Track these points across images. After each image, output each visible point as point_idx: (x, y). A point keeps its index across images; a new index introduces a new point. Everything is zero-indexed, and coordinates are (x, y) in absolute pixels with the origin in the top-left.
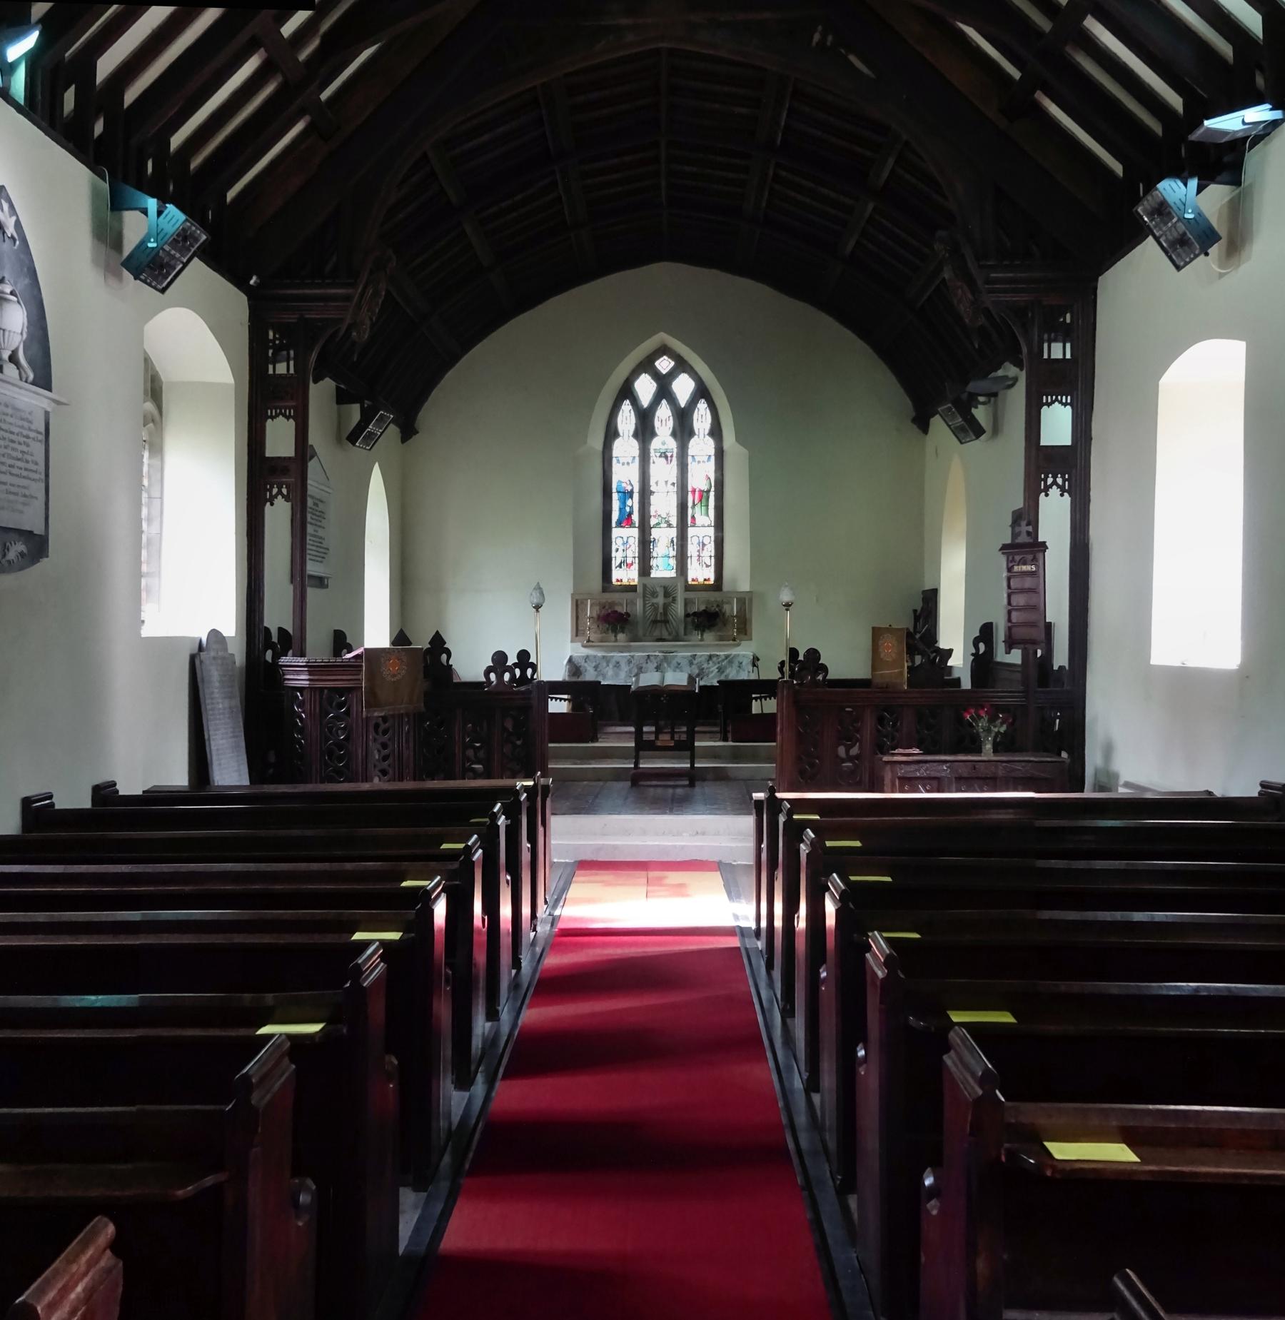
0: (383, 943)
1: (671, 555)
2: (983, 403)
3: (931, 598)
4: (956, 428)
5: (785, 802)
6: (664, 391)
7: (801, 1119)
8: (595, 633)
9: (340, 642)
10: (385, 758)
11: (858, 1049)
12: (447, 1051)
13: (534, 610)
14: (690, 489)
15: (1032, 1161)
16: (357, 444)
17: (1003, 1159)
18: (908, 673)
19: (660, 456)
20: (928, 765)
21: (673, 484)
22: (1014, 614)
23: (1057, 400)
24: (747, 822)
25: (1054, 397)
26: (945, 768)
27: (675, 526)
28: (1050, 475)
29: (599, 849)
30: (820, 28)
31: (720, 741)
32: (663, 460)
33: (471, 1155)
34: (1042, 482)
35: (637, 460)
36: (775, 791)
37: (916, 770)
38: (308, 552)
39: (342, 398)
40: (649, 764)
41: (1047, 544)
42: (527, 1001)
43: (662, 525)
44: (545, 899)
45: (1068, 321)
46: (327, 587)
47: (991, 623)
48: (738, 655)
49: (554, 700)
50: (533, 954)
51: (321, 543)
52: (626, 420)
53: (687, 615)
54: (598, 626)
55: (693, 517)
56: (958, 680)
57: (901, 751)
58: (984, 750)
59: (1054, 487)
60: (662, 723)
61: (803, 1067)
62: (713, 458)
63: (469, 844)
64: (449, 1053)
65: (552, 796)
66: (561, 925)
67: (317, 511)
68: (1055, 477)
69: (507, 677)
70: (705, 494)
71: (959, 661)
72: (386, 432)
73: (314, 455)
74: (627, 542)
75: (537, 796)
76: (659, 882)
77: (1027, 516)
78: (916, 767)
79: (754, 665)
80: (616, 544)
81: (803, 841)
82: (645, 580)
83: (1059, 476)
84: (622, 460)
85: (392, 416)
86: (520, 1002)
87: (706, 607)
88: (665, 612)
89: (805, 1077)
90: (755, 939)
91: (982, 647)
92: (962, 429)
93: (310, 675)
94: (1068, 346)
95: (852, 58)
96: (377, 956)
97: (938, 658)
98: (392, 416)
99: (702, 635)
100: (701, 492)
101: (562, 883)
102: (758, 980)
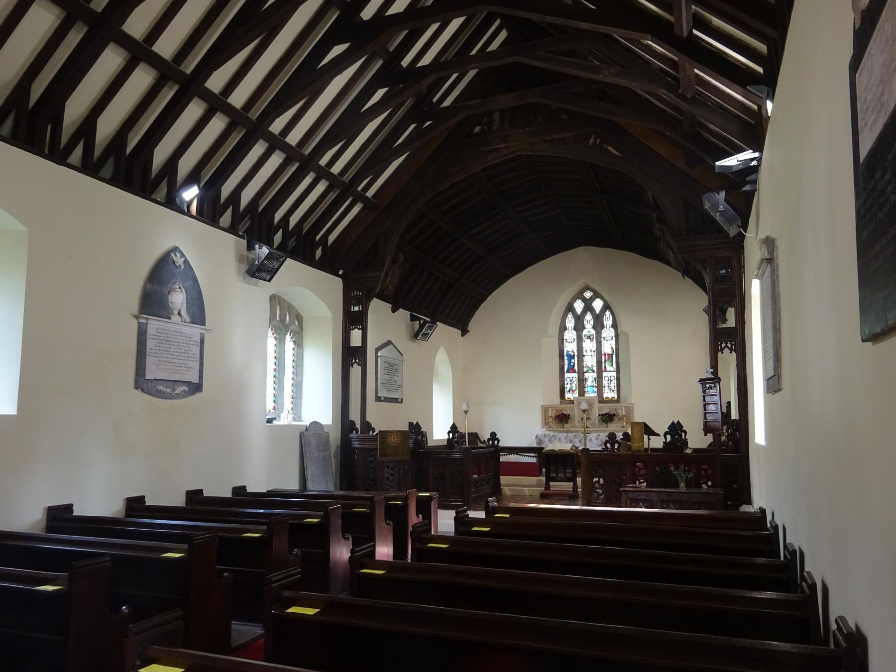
6: (588, 308)
19: (587, 338)
21: (594, 351)
32: (589, 340)
35: (576, 340)
55: (605, 367)
80: (568, 381)
84: (568, 341)
100: (608, 354)
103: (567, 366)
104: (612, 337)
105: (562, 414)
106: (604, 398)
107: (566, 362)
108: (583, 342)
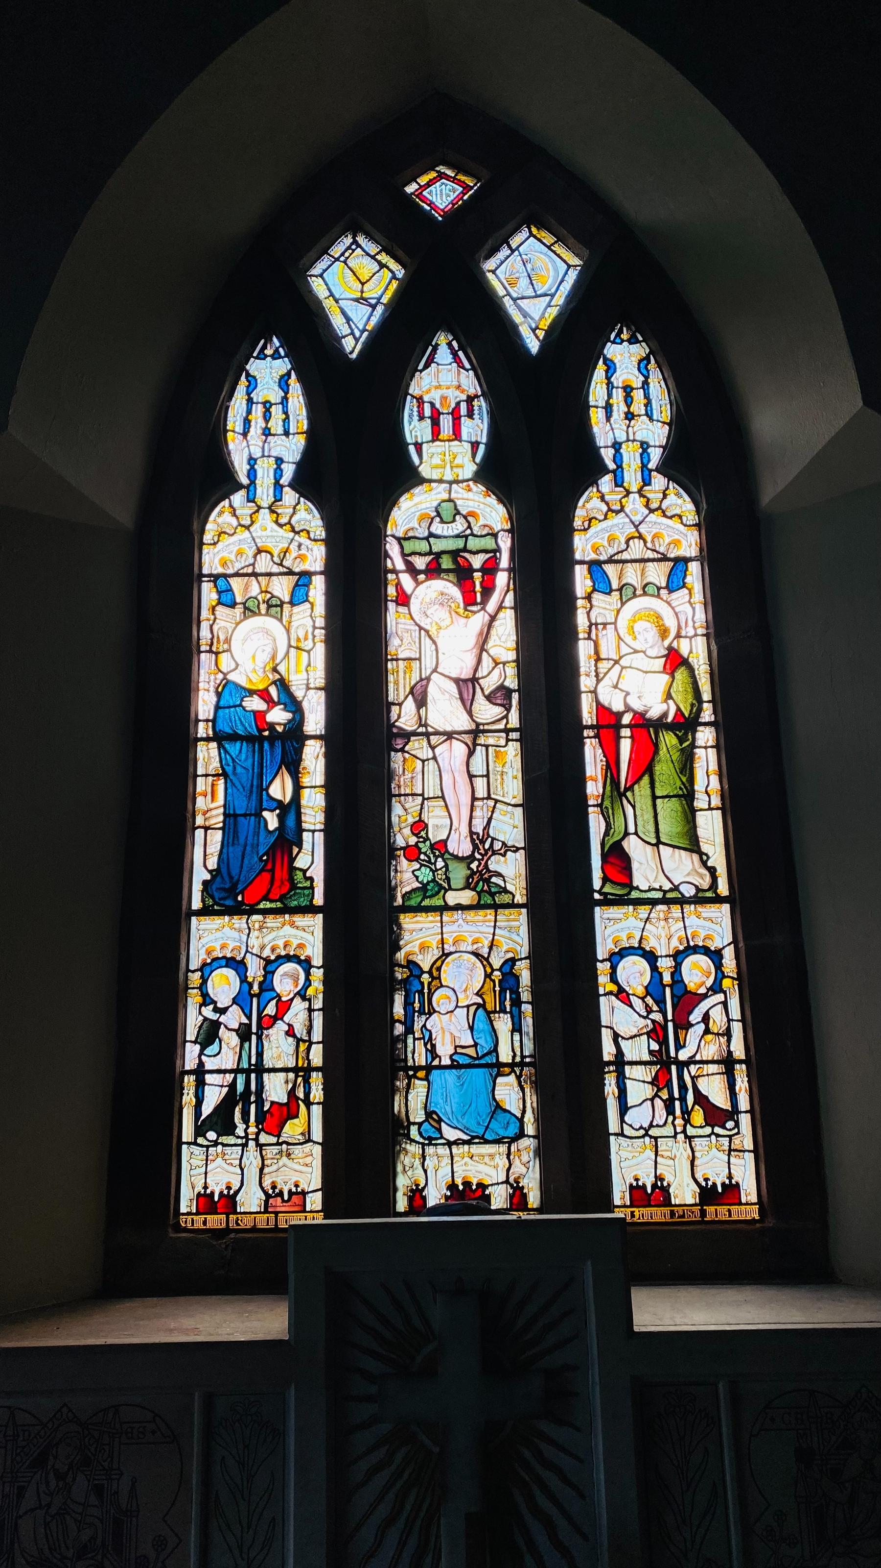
1: (505, 1056)
14: (588, 715)
27: (520, 899)
70: (669, 740)
103: (216, 837)
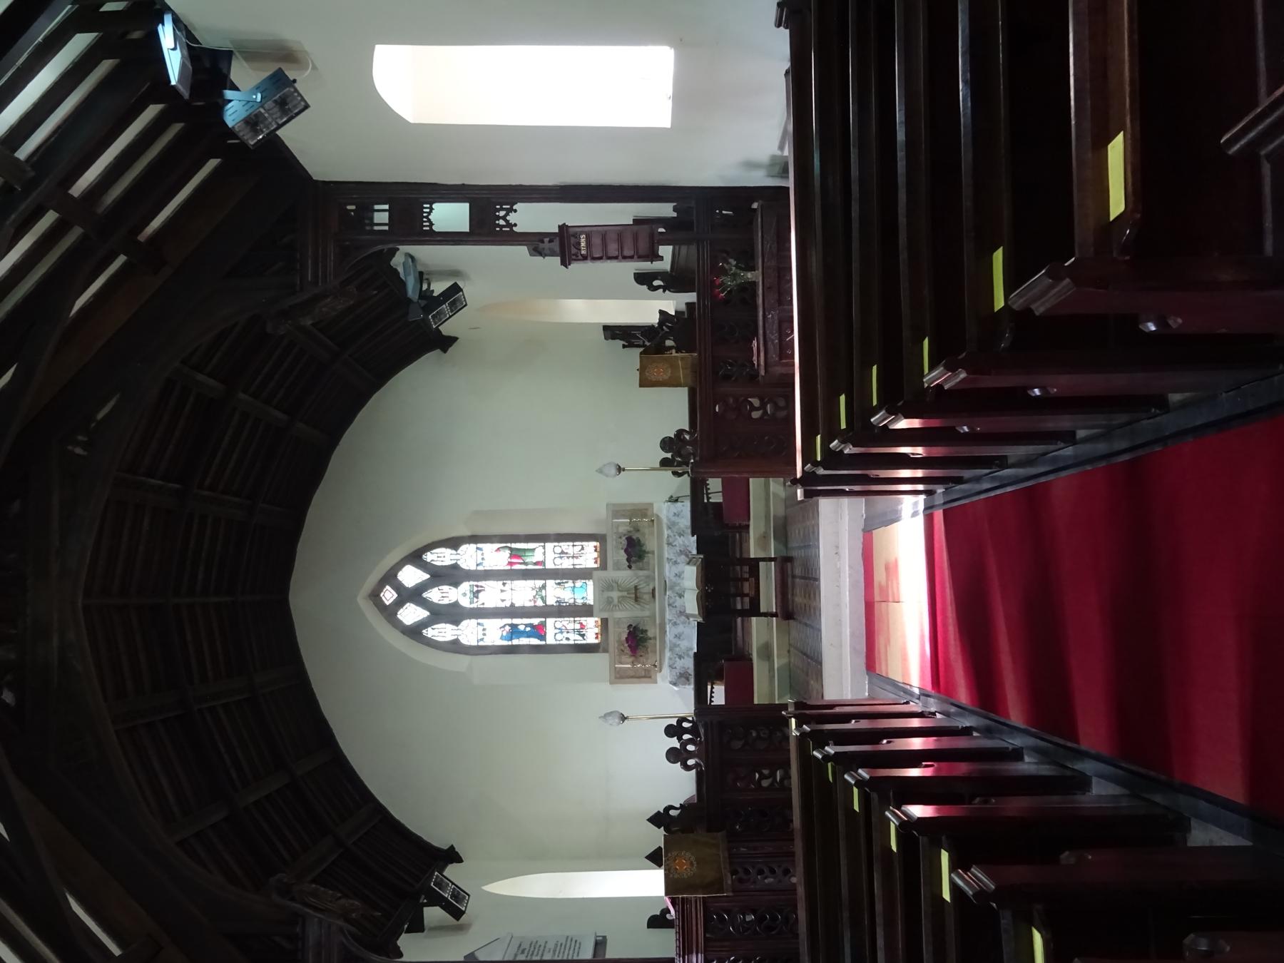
0: (952, 869)
1: (572, 585)
2: (429, 285)
3: (612, 332)
4: (452, 311)
5: (805, 468)
6: (414, 595)
7: (1102, 447)
8: (647, 659)
9: (658, 922)
10: (773, 872)
11: (1034, 395)
12: (1055, 801)
13: (626, 721)
14: (509, 568)
15: (1128, 232)
16: (463, 909)
17: (1127, 258)
18: (682, 353)
19: (477, 598)
20: (768, 332)
21: (504, 584)
22: (627, 253)
23: (427, 217)
24: (825, 504)
25: (425, 219)
26: (770, 316)
27: (544, 582)
28: (497, 222)
29: (853, 649)
30: (70, 448)
31: (749, 533)
32: (481, 595)
33: (1152, 773)
34: (504, 229)
35: (480, 621)
36: (796, 478)
37: (773, 343)
38: (570, 958)
39: (417, 926)
40: (769, 600)
41: (560, 224)
42: (1002, 720)
43: (544, 595)
44: (904, 704)
45: (353, 207)
46: (604, 937)
47: (635, 274)
48: (667, 517)
49: (713, 699)
50: (956, 714)
51: (561, 945)
52: (442, 632)
53: (630, 567)
54: (641, 656)
55: (537, 563)
56: (688, 304)
57: (755, 358)
58: (754, 280)
59: (508, 218)
60: (733, 590)
61: (1052, 447)
62: (480, 545)
63: (853, 782)
64: (1055, 798)
65: (805, 699)
66: (929, 688)
67: (529, 950)
68: (499, 218)
69: (691, 748)
70: (513, 553)
71: (672, 303)
72: (452, 880)
73: (472, 954)
74: (559, 629)
75: (805, 714)
76: (884, 591)
77: (536, 243)
78: (770, 343)
79: (676, 501)
80: (562, 639)
81: (841, 451)
82: (595, 610)
83: (497, 214)
84: (481, 636)
85: (436, 873)
86: (1005, 728)
87: (622, 549)
88: (628, 590)
89: (1062, 445)
90: (936, 495)
91: (656, 283)
92: (453, 305)
93: (692, 953)
94: (377, 207)
95: (100, 416)
96: (965, 876)
97: (667, 324)
98: (436, 873)
99: (648, 553)
100: (511, 556)
101: (888, 687)
102: (973, 492)
104: (477, 548)
105: (627, 642)
106: (596, 566)
107: (524, 641)
108: (485, 606)
